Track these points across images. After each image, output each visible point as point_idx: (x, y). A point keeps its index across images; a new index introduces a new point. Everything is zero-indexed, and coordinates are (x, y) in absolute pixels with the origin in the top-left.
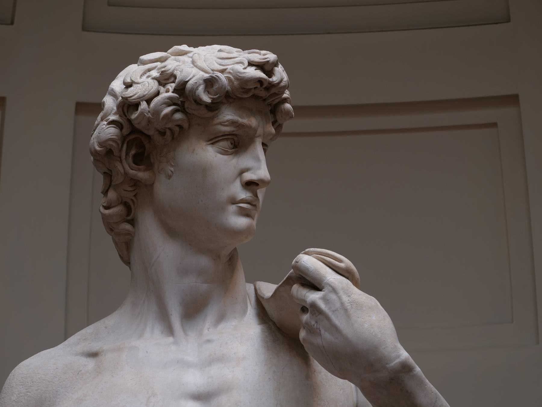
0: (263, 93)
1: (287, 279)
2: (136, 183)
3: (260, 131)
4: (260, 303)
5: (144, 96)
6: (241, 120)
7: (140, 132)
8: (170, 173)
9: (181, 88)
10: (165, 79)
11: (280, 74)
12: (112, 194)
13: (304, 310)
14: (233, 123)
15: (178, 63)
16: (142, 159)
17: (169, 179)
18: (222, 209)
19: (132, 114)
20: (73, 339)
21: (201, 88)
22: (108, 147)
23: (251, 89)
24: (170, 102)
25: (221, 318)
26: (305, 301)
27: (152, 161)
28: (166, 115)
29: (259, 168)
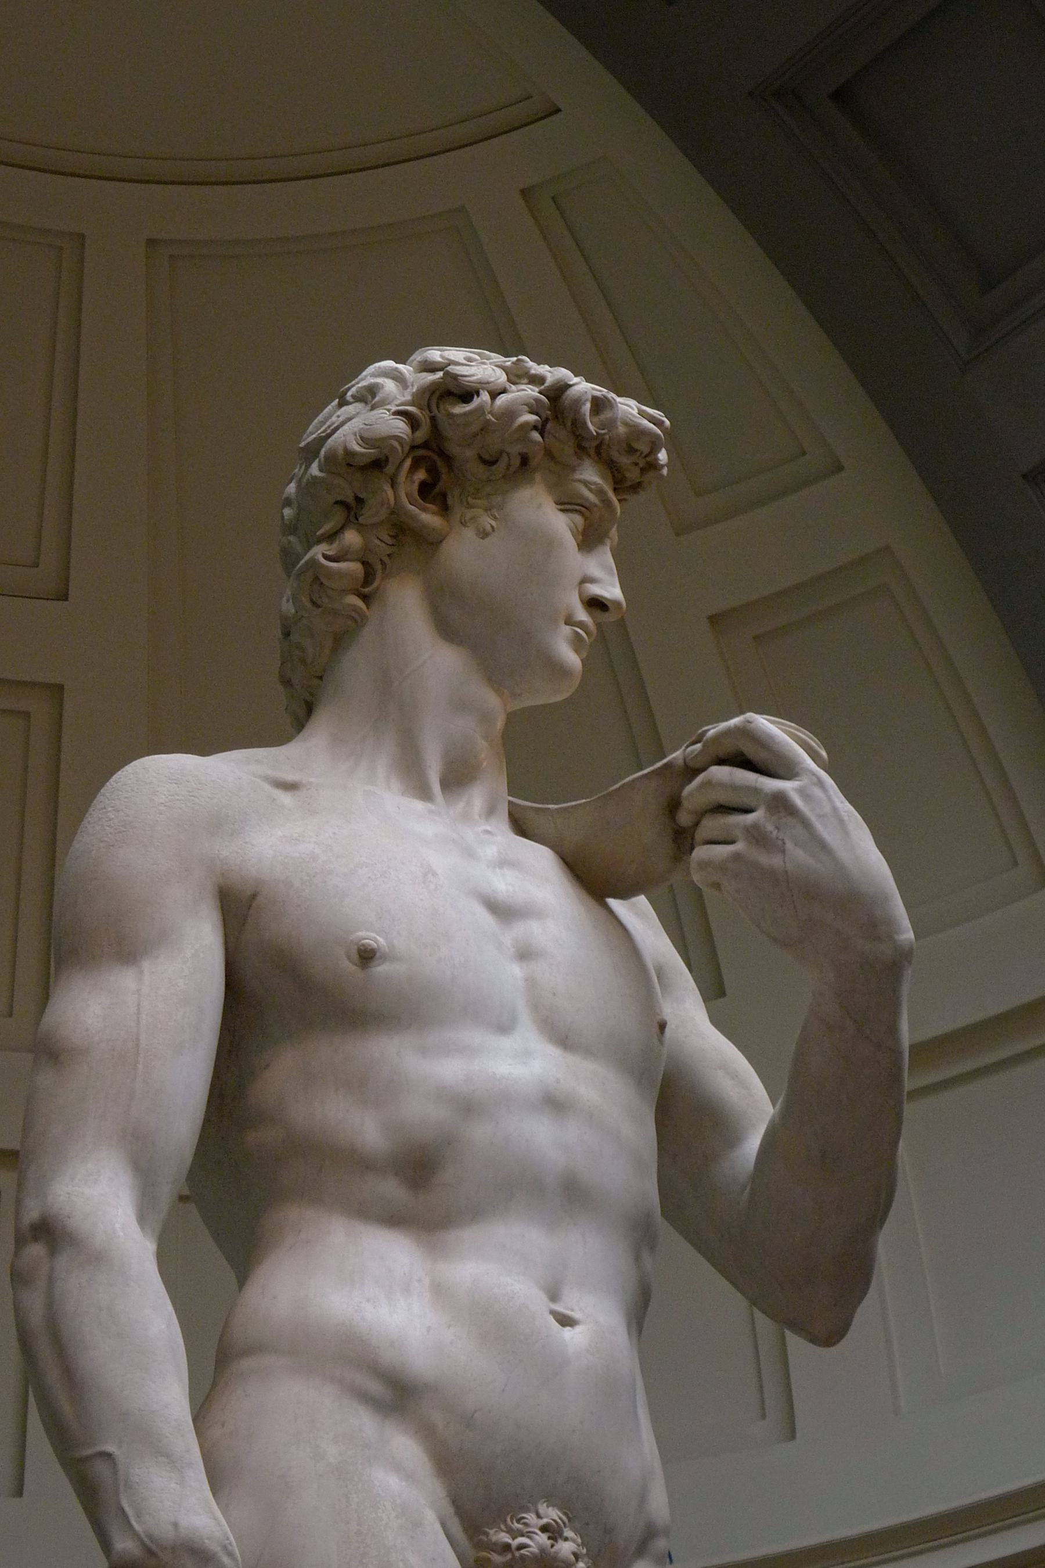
0: (633, 475)
1: (666, 765)
2: (402, 530)
5: (488, 383)
8: (488, 528)
9: (557, 393)
12: (351, 538)
14: (600, 492)
17: (483, 538)
19: (454, 405)
22: (386, 451)
23: (637, 450)
25: (490, 812)
26: (756, 791)
27: (450, 501)
28: (527, 423)
29: (613, 586)
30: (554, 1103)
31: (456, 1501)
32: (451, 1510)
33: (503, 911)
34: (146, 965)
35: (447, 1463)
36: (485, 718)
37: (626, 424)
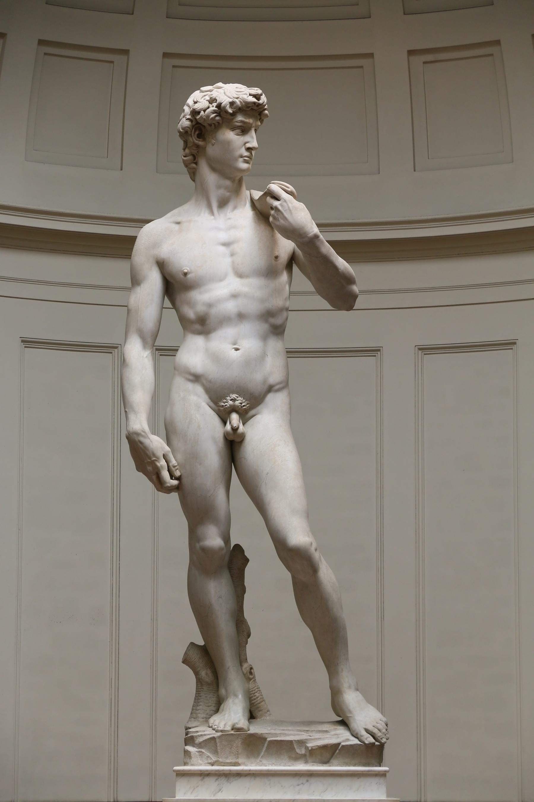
0: (255, 108)
2: (198, 146)
3: (254, 125)
4: (252, 200)
6: (245, 120)
7: (200, 124)
9: (219, 106)
10: (212, 101)
11: (264, 99)
12: (187, 151)
13: (272, 208)
14: (242, 122)
15: (218, 93)
16: (201, 136)
18: (236, 160)
20: (169, 215)
21: (228, 106)
24: (214, 112)
25: (235, 208)
28: (212, 118)
29: (253, 142)
30: (234, 296)
31: (211, 398)
32: (210, 401)
33: (226, 244)
34: (142, 285)
35: (208, 391)
36: (226, 188)
37: (244, 102)
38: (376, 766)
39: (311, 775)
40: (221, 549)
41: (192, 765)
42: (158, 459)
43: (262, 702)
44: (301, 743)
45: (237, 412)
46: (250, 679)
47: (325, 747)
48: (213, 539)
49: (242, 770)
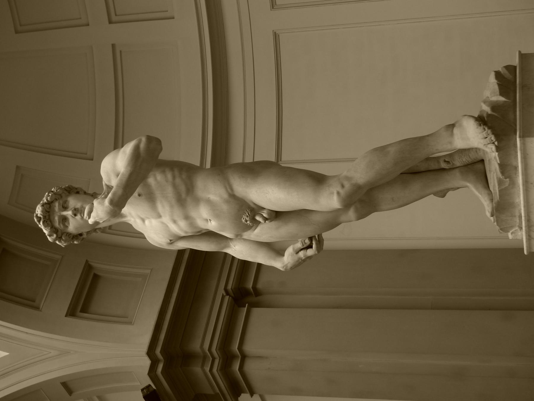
3: (59, 214)
6: (57, 223)
14: (59, 224)
30: (175, 222)
38: (516, 139)
39: (526, 182)
40: (357, 211)
41: (522, 238)
42: (300, 258)
43: (470, 157)
44: (500, 182)
45: (254, 216)
46: (453, 164)
47: (503, 173)
48: (351, 213)
49: (525, 220)
